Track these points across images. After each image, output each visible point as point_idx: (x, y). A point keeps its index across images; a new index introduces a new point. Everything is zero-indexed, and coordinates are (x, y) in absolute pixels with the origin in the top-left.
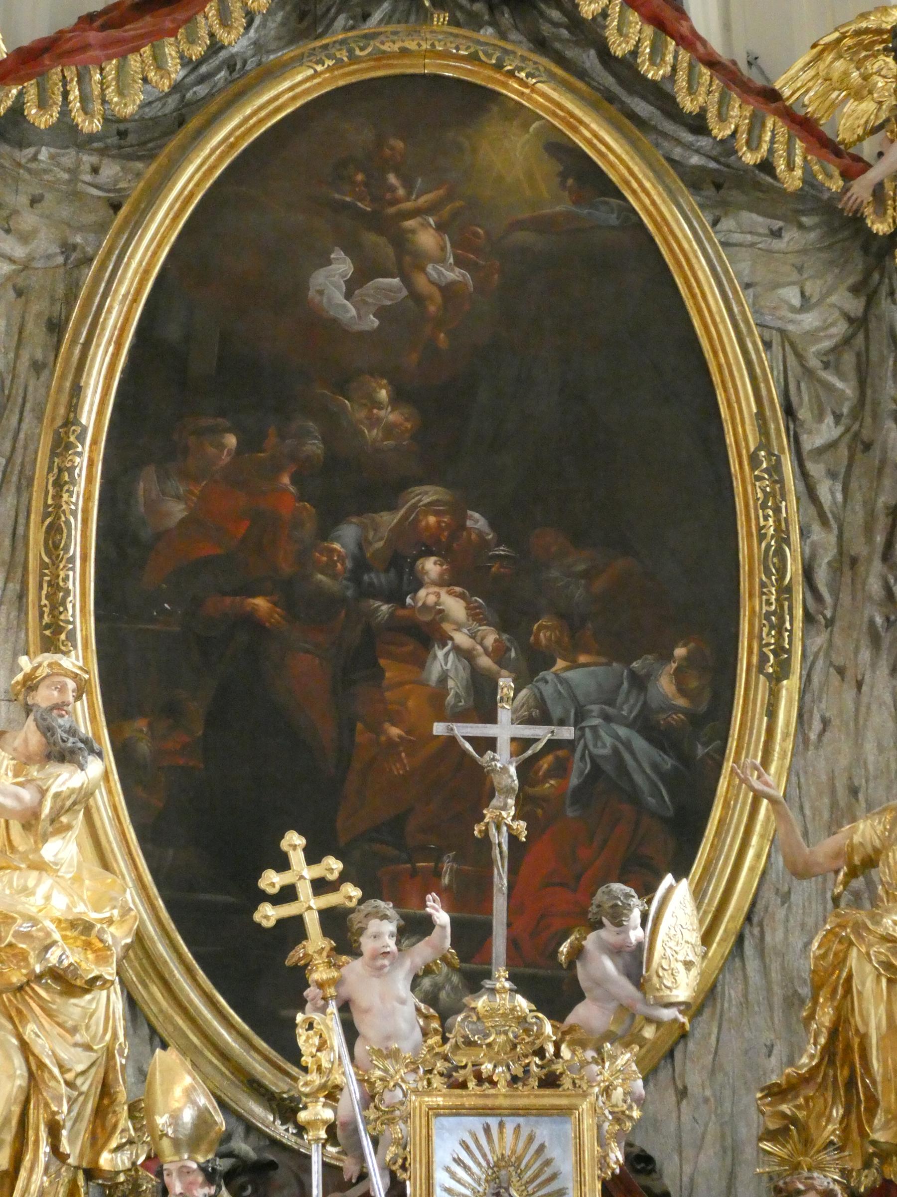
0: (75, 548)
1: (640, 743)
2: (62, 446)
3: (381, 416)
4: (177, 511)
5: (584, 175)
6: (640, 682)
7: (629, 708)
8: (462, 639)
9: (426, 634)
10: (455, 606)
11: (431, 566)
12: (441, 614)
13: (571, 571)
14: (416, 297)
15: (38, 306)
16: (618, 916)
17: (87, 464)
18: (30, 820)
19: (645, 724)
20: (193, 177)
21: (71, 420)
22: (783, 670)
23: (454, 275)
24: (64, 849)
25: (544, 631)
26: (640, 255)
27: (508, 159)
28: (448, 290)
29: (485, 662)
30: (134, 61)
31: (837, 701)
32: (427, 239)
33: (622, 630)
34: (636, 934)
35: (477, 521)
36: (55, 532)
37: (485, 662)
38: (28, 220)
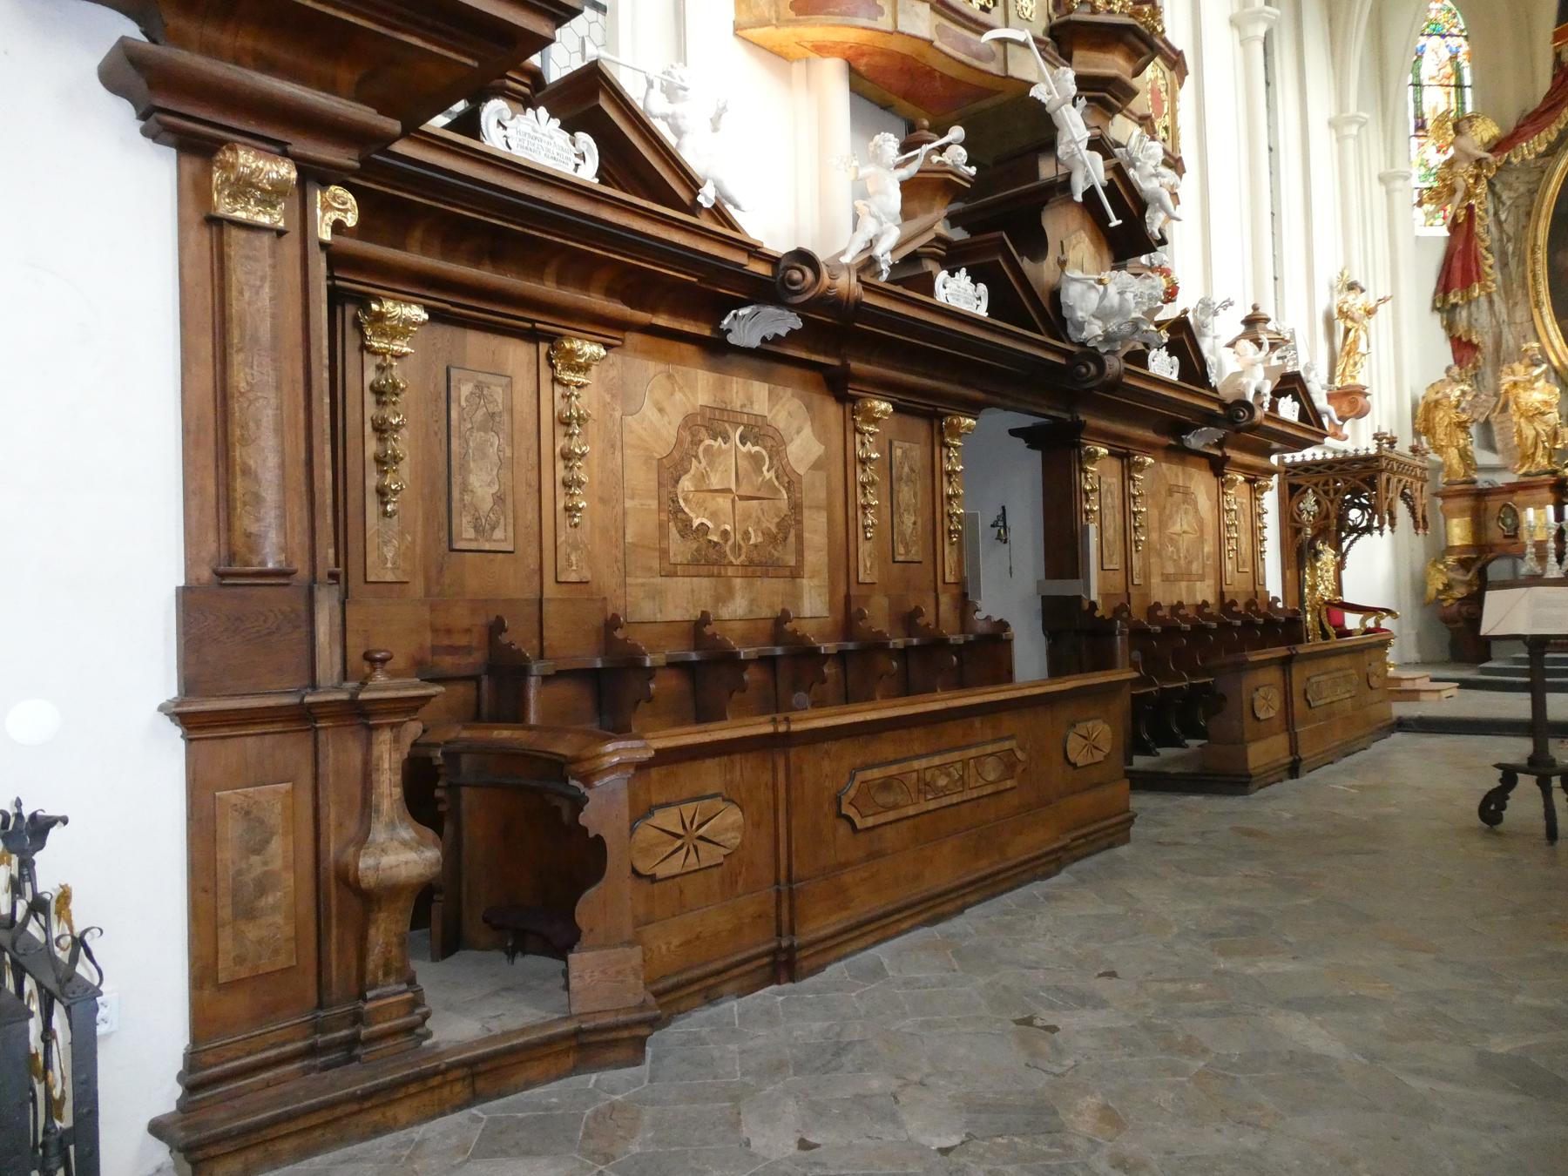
2: (1533, 252)
15: (1522, 210)
17: (1542, 255)
24: (1541, 384)
38: (1516, 185)
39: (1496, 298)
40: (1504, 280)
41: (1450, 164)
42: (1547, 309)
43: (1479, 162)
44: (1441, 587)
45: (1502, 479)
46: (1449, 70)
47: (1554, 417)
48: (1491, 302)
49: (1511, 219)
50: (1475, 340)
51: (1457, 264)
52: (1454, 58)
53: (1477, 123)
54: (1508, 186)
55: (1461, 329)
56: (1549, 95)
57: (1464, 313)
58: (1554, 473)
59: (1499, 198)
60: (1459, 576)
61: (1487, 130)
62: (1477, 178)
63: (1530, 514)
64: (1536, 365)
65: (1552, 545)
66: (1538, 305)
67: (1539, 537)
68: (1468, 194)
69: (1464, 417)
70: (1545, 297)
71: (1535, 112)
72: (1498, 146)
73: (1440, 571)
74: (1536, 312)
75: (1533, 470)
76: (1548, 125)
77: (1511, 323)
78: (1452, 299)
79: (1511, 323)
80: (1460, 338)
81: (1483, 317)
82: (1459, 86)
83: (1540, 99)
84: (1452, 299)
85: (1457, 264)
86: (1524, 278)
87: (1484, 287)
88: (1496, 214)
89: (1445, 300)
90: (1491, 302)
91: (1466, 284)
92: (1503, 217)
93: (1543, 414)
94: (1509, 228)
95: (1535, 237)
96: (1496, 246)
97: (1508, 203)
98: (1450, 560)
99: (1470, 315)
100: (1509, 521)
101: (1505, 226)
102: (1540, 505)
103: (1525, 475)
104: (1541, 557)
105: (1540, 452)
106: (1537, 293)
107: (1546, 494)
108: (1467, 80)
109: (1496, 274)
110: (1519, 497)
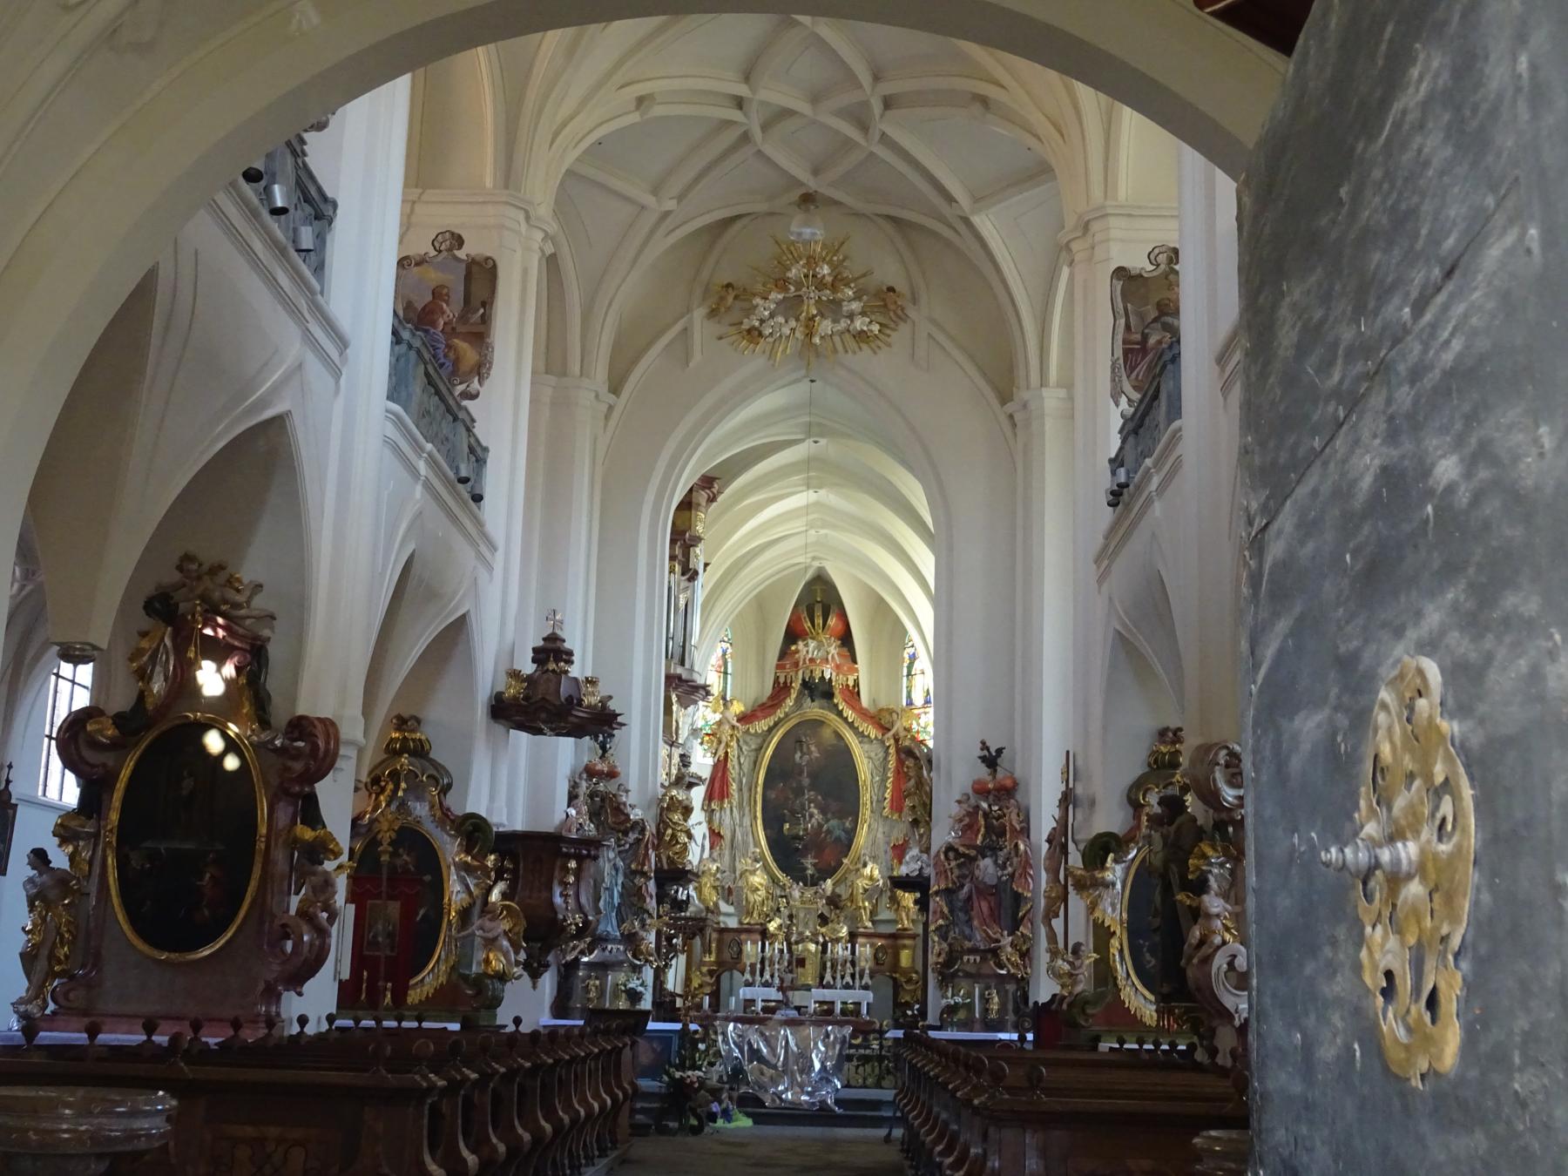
3: (806, 781)
5: (839, 736)
9: (811, 816)
17: (760, 789)
26: (847, 752)
27: (827, 733)
31: (874, 826)
33: (841, 815)
41: (719, 723)
42: (759, 822)
43: (733, 727)
45: (733, 923)
47: (762, 893)
52: (724, 653)
54: (746, 743)
56: (772, 698)
60: (708, 979)
61: (737, 708)
63: (748, 947)
64: (757, 861)
68: (727, 745)
70: (759, 814)
72: (744, 718)
82: (726, 673)
83: (765, 699)
85: (717, 785)
94: (746, 768)
98: (705, 969)
102: (754, 943)
104: (753, 973)
107: (758, 937)
109: (736, 795)
110: (743, 937)
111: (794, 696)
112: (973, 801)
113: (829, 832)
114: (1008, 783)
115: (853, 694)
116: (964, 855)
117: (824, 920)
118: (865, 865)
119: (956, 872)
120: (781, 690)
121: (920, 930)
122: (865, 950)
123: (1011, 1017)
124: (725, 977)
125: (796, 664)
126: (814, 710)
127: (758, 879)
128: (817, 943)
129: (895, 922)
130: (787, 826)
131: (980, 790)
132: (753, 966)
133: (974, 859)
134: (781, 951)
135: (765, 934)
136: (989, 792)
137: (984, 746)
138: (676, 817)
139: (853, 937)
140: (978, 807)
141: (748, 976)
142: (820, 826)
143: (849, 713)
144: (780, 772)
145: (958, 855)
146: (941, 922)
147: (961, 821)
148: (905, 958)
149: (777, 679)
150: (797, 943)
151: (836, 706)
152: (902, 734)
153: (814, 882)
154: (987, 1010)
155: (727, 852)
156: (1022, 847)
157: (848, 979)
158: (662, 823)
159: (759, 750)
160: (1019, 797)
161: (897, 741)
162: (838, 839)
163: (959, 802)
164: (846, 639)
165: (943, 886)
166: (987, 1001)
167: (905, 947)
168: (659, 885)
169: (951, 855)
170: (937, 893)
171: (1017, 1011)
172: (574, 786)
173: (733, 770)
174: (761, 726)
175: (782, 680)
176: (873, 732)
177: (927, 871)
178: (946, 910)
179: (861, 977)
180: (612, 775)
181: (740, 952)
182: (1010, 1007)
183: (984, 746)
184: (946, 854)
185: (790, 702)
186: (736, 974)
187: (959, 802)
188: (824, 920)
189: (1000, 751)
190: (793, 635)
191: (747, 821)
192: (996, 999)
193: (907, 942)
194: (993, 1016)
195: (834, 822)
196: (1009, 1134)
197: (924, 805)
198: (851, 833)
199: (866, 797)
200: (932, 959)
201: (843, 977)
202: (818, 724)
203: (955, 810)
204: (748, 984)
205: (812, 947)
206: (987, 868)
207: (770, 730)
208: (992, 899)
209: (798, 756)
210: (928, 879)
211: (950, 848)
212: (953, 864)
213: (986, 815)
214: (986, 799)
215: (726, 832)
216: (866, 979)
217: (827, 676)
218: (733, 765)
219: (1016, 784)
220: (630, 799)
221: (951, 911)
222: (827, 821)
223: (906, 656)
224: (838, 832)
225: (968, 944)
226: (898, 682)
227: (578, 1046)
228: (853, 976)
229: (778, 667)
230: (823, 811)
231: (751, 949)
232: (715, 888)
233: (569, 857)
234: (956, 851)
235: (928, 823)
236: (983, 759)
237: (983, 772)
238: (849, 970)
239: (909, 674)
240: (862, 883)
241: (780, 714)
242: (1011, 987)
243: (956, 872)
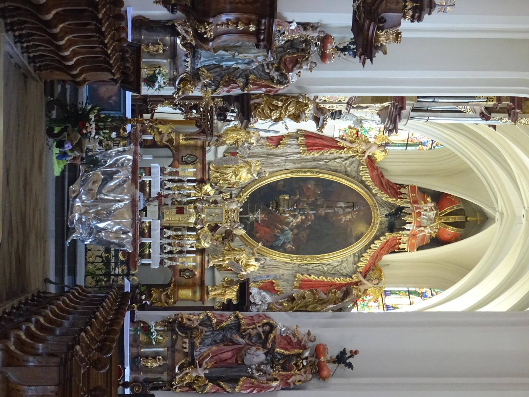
0: (303, 174)
1: (282, 242)
2: (317, 172)
4: (310, 186)
5: (358, 238)
6: (289, 242)
7: (286, 241)
8: (294, 221)
9: (295, 216)
10: (298, 220)
11: (304, 217)
12: (297, 218)
13: (304, 235)
14: (340, 215)
16: (240, 226)
17: (315, 175)
18: (251, 172)
19: (284, 243)
20: (354, 187)
21: (320, 173)
22: (291, 260)
23: (343, 220)
25: (295, 231)
26: (346, 244)
27: (361, 228)
28: (341, 220)
29: (291, 224)
30: (370, 179)
31: (288, 267)
32: (348, 217)
33: (296, 240)
34: (239, 227)
35: (310, 223)
36: (306, 172)
37: (291, 224)
39: (299, 155)
40: (307, 159)
41: (367, 142)
42: (289, 176)
43: (364, 153)
44: (160, 130)
45: (209, 156)
46: (416, 141)
47: (234, 179)
48: (298, 153)
49: (335, 163)
50: (279, 146)
51: (317, 141)
52: (422, 144)
53: (384, 153)
54: (351, 164)
55: (285, 141)
57: (294, 142)
58: (209, 179)
59: (347, 159)
60: (166, 138)
61: (379, 156)
62: (357, 151)
64: (259, 174)
65: (177, 178)
66: (292, 172)
67: (181, 173)
68: (349, 148)
69: (240, 144)
70: (295, 175)
71: (383, 176)
72: (371, 161)
73: (168, 130)
74: (289, 171)
75: (211, 172)
76: (374, 181)
77: (286, 161)
78: (300, 138)
79: (286, 161)
80: (282, 140)
81: (290, 150)
82: (407, 145)
83: (386, 177)
84: (300, 138)
85: (317, 141)
86: (306, 168)
87: (304, 152)
88: (339, 158)
89: (301, 135)
90: (298, 153)
91: (307, 145)
92: (337, 160)
93: (236, 176)
95: (324, 174)
96: (322, 157)
97: (344, 163)
98: (173, 136)
99: (292, 145)
100: (189, 159)
101: (333, 161)
102: (195, 174)
103: (209, 168)
104: (171, 173)
105: (218, 174)
106: (298, 172)
107: (199, 177)
108: (408, 148)
109: (310, 156)
110: (199, 165)
111: (390, 200)
112: (310, 344)
113: (283, 231)
114: (325, 373)
115: (393, 248)
116: (267, 338)
117: (214, 228)
118: (257, 260)
119: (254, 332)
120: (395, 190)
121: (208, 304)
122: (190, 261)
123: (142, 376)
124: (167, 152)
125: (415, 202)
126: (380, 217)
127: (244, 176)
128: (195, 224)
129: (214, 285)
130: (287, 197)
131: (318, 351)
132: (177, 173)
133: (264, 347)
134: (189, 196)
135: (202, 182)
136: (318, 357)
137: (354, 353)
138: (291, 109)
139: (202, 251)
140: (305, 348)
141: (169, 170)
142: (287, 224)
143: (378, 244)
144: (329, 191)
145: (267, 334)
146: (214, 320)
147: (294, 335)
148: (185, 293)
149: (403, 186)
150: (195, 208)
151: (383, 234)
152: (362, 288)
153: (243, 220)
154: (147, 358)
155: (265, 150)
156: (275, 384)
157: (168, 249)
158: (286, 98)
159: (347, 174)
160: (314, 381)
161: (356, 284)
162: (277, 238)
163: (309, 334)
164: (437, 241)
165: (242, 321)
166: (154, 358)
167: (194, 293)
168: (238, 98)
169: (267, 328)
170: (237, 317)
171: (147, 381)
172: (314, 27)
173: (329, 154)
174: (366, 176)
175: (403, 191)
176: (363, 264)
177: (254, 309)
178: (224, 324)
179: (170, 259)
180: (324, 57)
181: (188, 163)
182: (150, 376)
183: (354, 353)
184: (268, 324)
185: (385, 197)
186: (171, 160)
187: (309, 334)
188: (214, 228)
189: (350, 365)
190: (439, 198)
191: (290, 166)
192: (155, 365)
193: (198, 295)
194: (143, 363)
195: (290, 235)
196: (54, 373)
197: (306, 306)
198: (282, 249)
199: (311, 260)
200: (185, 314)
201: (169, 244)
202: (369, 221)
203: (303, 331)
204: (162, 170)
205: (192, 220)
206: (257, 356)
207: (362, 182)
208: (233, 360)
209: (342, 205)
210: (247, 310)
211: (272, 327)
212: (260, 330)
213: (299, 355)
214: (311, 355)
215: (280, 149)
216: (168, 263)
217: (407, 227)
218: (334, 153)
219: (324, 378)
220: (305, 73)
221: (223, 329)
222: (292, 230)
223: (425, 290)
224: (282, 238)
225: (197, 342)
226: (404, 284)
227: (112, 38)
228: (171, 252)
229: (413, 187)
230: (299, 226)
231: (189, 172)
232: (237, 142)
233: (258, 25)
234: (270, 332)
235: (291, 309)
236: (343, 353)
237: (333, 352)
238: (175, 249)
239: (409, 293)
240: (243, 257)
241: (376, 190)
242: (165, 376)
243: (254, 332)
